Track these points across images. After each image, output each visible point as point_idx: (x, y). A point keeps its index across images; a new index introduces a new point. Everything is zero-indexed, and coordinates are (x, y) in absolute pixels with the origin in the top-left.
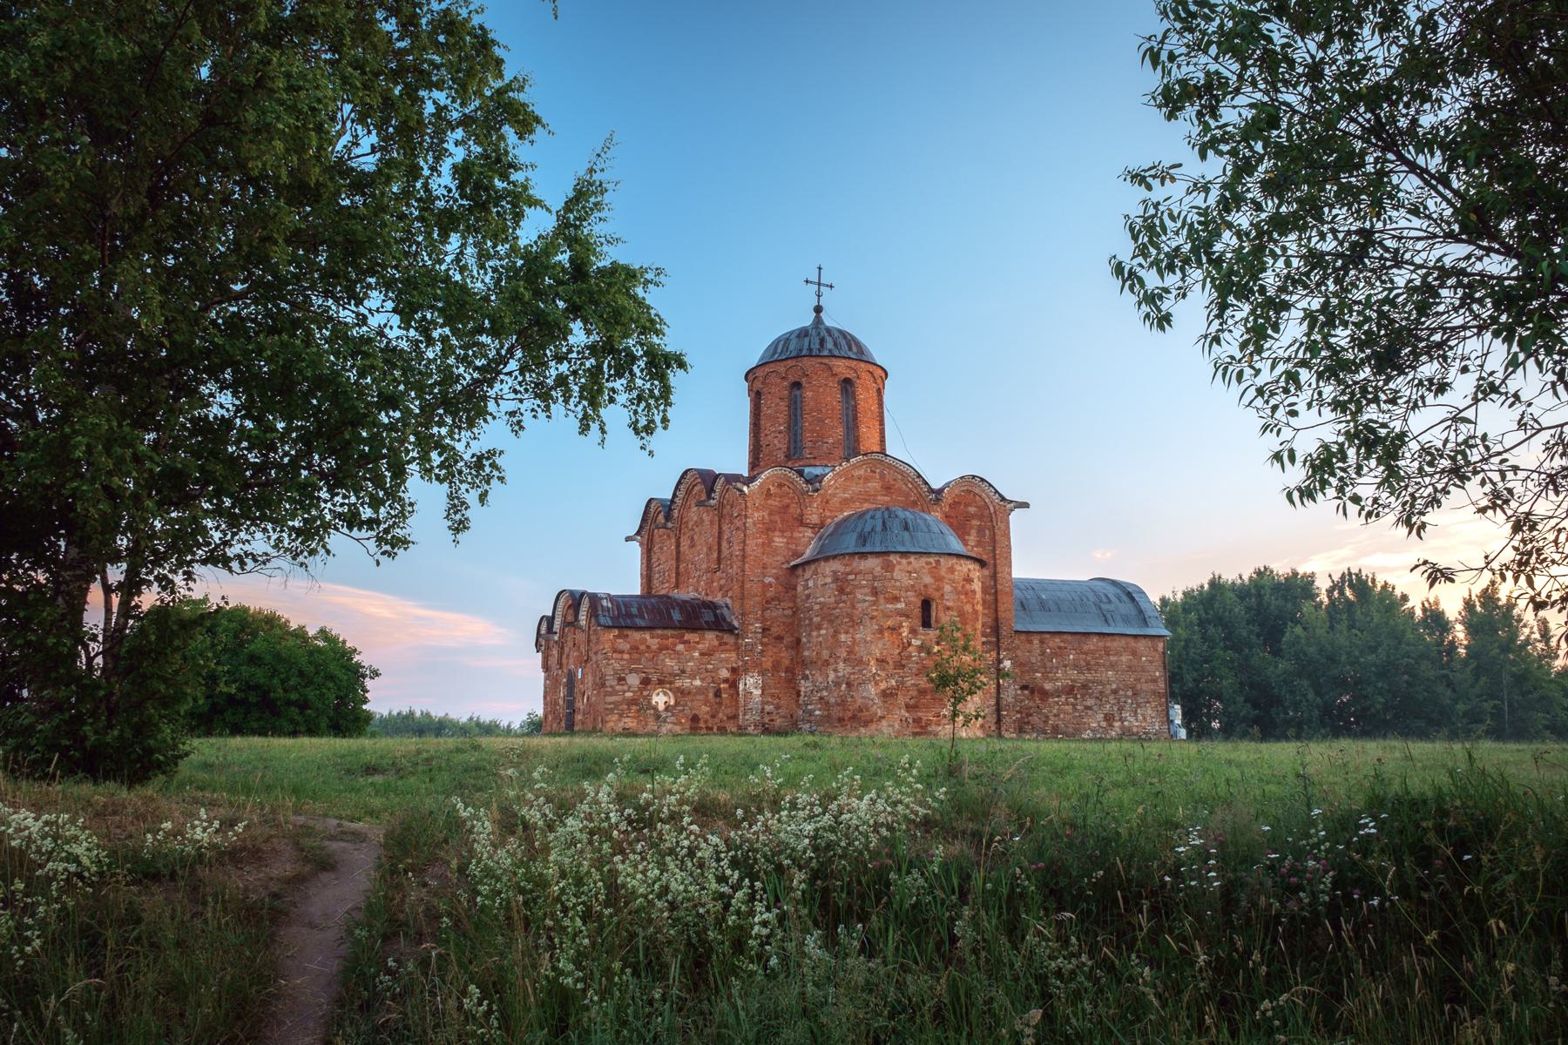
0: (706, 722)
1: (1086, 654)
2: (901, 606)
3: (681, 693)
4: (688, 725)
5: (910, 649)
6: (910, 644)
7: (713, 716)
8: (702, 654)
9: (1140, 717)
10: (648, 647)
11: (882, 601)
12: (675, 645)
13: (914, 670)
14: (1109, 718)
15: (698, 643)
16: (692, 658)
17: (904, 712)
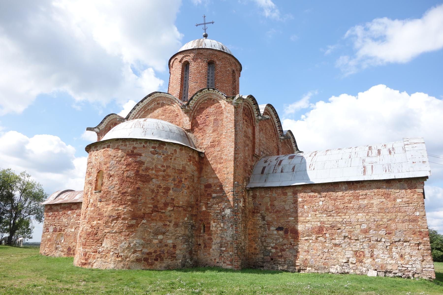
1: (335, 200)
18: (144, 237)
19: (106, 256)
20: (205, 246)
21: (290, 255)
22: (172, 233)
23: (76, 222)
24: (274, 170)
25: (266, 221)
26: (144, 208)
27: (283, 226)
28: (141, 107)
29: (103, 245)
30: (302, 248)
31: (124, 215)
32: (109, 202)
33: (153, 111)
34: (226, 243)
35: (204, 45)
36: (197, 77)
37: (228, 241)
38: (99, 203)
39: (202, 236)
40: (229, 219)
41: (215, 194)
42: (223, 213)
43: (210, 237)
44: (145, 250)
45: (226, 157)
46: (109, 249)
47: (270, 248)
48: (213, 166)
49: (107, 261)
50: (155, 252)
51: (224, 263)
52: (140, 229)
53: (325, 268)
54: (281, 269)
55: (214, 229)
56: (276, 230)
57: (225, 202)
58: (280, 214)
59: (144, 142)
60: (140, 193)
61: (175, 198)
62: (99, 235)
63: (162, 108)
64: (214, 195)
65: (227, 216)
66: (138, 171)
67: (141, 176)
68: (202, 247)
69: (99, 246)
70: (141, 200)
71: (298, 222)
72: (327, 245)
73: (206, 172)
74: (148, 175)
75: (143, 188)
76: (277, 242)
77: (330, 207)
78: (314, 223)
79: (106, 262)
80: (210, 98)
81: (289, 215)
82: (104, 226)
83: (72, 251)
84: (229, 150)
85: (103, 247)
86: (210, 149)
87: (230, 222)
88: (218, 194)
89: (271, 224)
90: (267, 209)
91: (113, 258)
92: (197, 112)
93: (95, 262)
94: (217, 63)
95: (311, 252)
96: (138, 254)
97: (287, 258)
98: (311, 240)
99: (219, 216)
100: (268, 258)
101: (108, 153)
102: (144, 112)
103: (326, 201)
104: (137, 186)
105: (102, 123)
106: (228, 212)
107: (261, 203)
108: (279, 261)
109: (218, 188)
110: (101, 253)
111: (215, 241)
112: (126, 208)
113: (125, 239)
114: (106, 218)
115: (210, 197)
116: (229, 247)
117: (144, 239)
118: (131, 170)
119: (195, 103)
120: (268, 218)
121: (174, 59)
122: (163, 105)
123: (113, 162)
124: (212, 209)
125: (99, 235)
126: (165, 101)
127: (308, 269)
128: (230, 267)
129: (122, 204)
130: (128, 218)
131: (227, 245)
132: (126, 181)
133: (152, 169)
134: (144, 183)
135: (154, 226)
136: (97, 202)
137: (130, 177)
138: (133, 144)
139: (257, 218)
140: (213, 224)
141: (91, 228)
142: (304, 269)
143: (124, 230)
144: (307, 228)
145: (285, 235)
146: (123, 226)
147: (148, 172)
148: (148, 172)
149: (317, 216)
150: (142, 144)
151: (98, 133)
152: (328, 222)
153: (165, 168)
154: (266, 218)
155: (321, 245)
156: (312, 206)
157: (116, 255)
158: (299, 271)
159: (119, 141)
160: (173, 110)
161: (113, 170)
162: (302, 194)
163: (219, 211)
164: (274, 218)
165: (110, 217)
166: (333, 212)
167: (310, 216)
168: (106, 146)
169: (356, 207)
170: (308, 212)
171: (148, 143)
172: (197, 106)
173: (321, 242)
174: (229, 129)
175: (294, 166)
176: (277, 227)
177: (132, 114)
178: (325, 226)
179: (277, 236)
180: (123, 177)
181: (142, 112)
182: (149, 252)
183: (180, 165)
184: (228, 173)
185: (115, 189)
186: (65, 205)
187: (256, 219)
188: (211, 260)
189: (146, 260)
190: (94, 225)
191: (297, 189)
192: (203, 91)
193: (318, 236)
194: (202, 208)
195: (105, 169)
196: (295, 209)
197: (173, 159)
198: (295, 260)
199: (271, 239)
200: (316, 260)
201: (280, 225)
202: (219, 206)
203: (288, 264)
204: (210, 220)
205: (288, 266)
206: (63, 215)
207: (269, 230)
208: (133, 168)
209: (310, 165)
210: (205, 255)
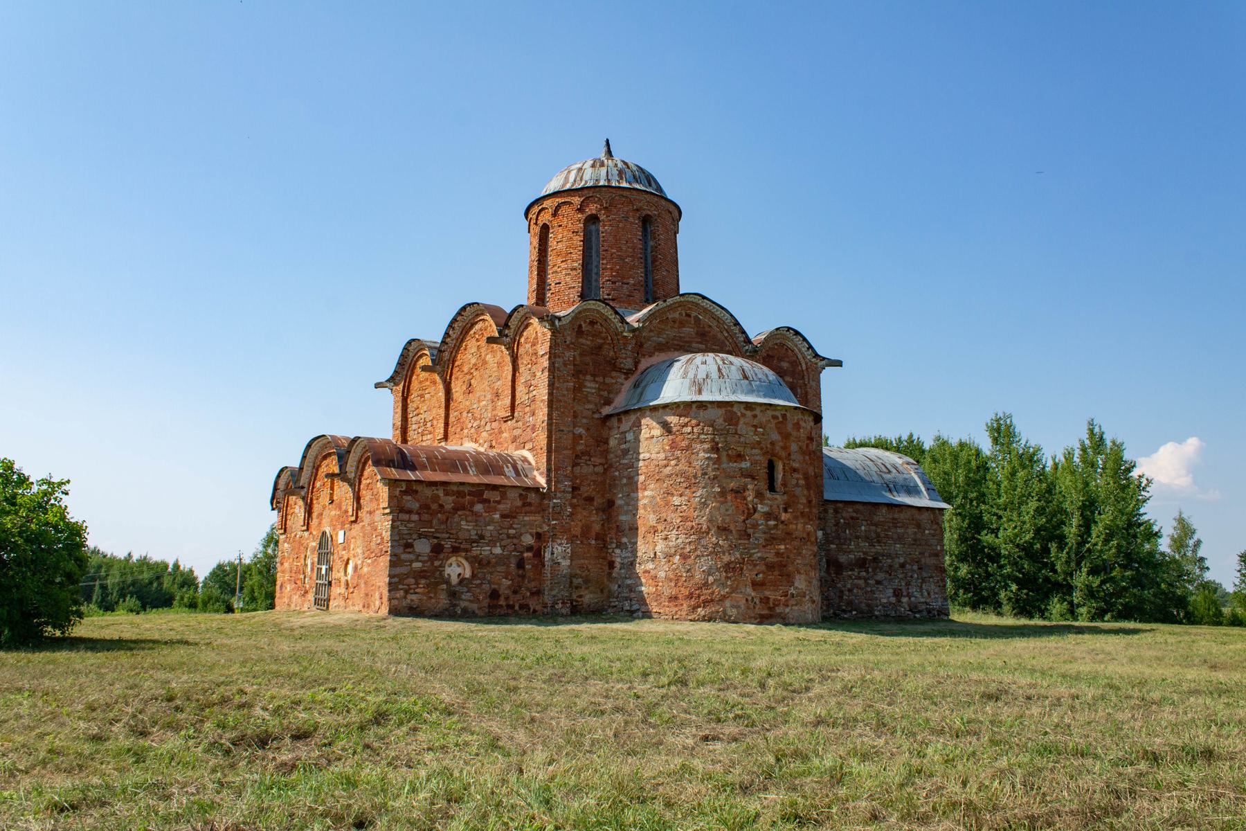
0: (507, 598)
1: (876, 525)
2: (745, 465)
3: (477, 562)
4: (486, 602)
5: (756, 516)
6: (755, 510)
7: (515, 592)
8: (503, 516)
9: (926, 594)
10: (441, 506)
11: (724, 459)
12: (472, 504)
14: (897, 593)
15: (499, 502)
16: (492, 521)
38: (783, 514)
83: (502, 598)
167: (853, 543)
169: (895, 536)
170: (850, 540)
186: (461, 488)
206: (459, 513)
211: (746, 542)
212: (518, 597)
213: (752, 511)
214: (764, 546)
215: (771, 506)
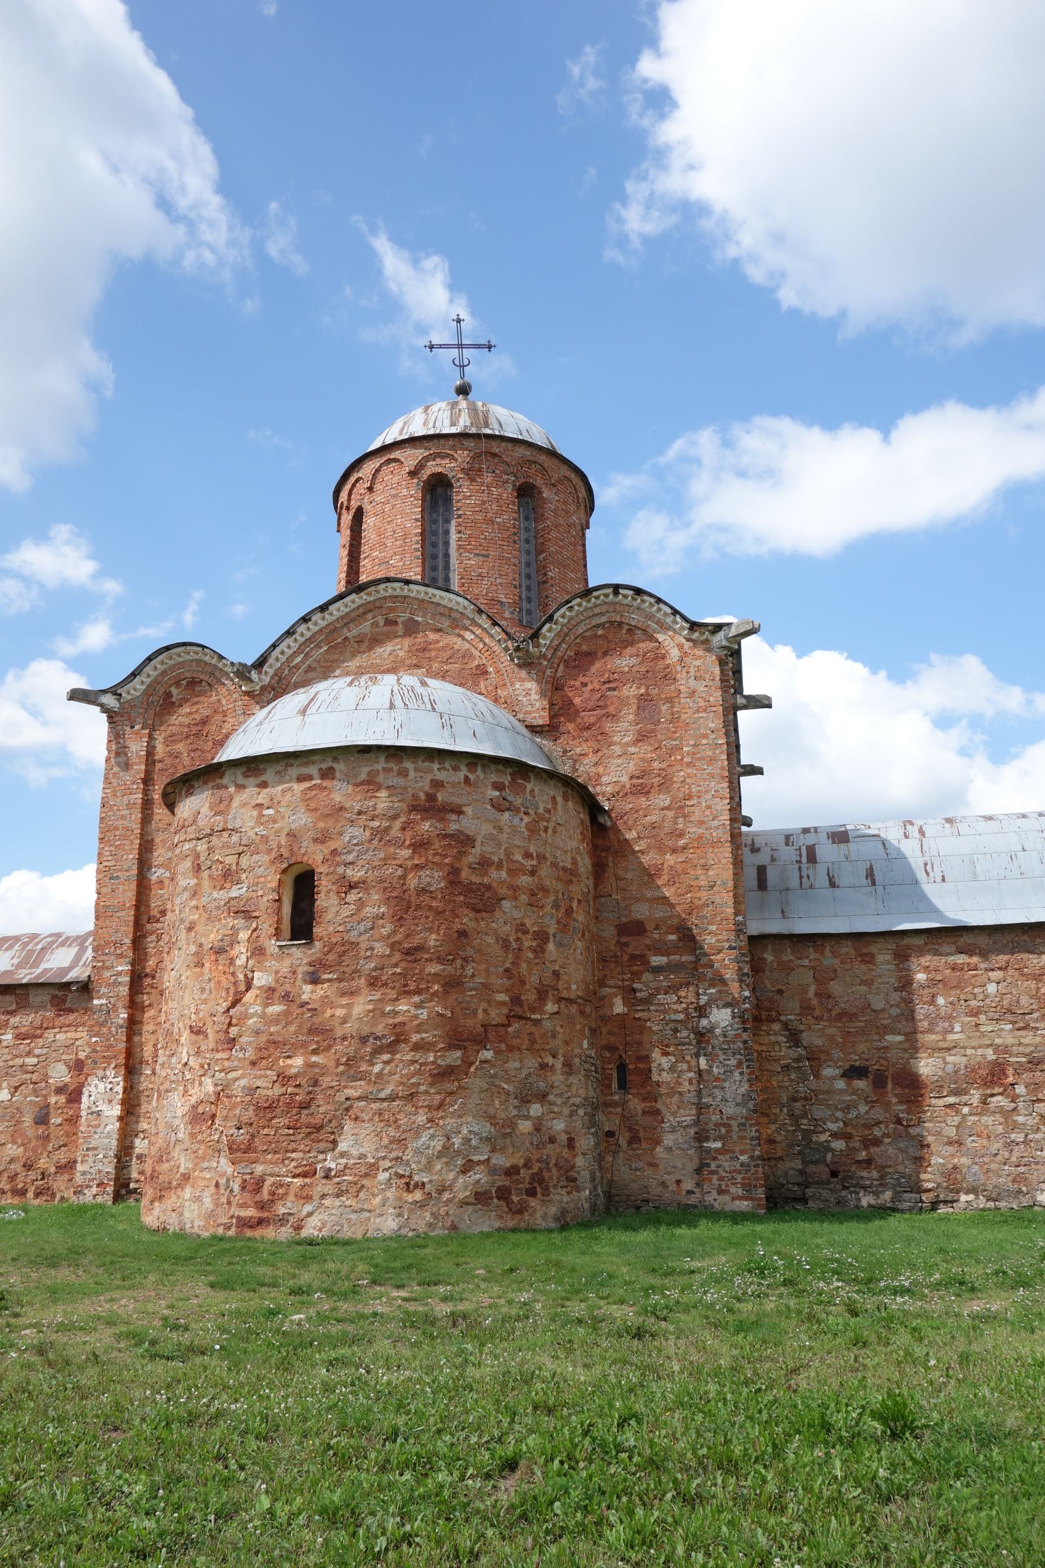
5: (249, 997)
7: (28, 1166)
8: (18, 1037)
11: (206, 884)
13: (250, 1054)
17: (225, 1165)
18: (491, 1110)
19: (363, 1186)
20: (634, 1139)
21: (898, 1157)
22: (561, 1095)
23: (18, 1061)
24: (801, 877)
25: (805, 1048)
26: (484, 1005)
27: (868, 1063)
28: (315, 629)
29: (342, 1146)
30: (938, 1133)
31: (418, 1032)
32: (354, 983)
33: (370, 649)
34: (724, 1125)
35: (496, 426)
36: (485, 539)
37: (728, 1118)
38: (308, 988)
39: (615, 1104)
40: (728, 1043)
41: (663, 955)
42: (704, 1022)
43: (651, 1107)
44: (500, 1160)
45: (700, 831)
46: (372, 1161)
47: (823, 1138)
48: (646, 859)
49: (365, 1207)
50: (527, 1165)
51: (721, 1192)
52: (475, 1082)
53: (1020, 1191)
54: (870, 1206)
55: (666, 1077)
56: (842, 1076)
57: (707, 984)
58: (854, 1025)
59: (467, 765)
60: (470, 952)
61: (562, 971)
62: (322, 1109)
63: (407, 641)
64: (657, 960)
65: (718, 1031)
66: (455, 871)
67: (468, 889)
68: (623, 1142)
69: (322, 1152)
70: (473, 976)
71: (917, 1050)
72: (1020, 1119)
73: (618, 879)
74: (489, 887)
75: (478, 933)
76: (850, 1116)
77: (1025, 1001)
78: (973, 1051)
79: (362, 1210)
80: (618, 619)
81: (885, 1027)
82: (343, 1073)
84: (709, 807)
85: (343, 1155)
86: (630, 798)
87: (734, 1054)
88: (672, 957)
89: (823, 1057)
90: (806, 1009)
91: (391, 1194)
92: (566, 667)
93: (310, 1214)
94: (545, 495)
95: (969, 1145)
96: (478, 1175)
97: (890, 1166)
98: (965, 1104)
99: (685, 1033)
100: (823, 1171)
101: (332, 796)
102: (326, 648)
103: (1009, 980)
104: (457, 926)
105: (134, 675)
106: (721, 1017)
107: (784, 988)
108: (862, 1178)
109: (673, 937)
110: (335, 1176)
111: (671, 1119)
112: (424, 1008)
113: (430, 1120)
114: (349, 1046)
115: (640, 968)
116: (735, 1137)
117: (491, 1118)
118: (430, 865)
119: (558, 635)
120: (813, 1038)
121: (385, 459)
122: (411, 629)
123: (355, 833)
124: (652, 1008)
125: (322, 1109)
126: (421, 614)
127: (964, 1198)
128: (745, 1205)
129: (408, 993)
130: (433, 1044)
131: (728, 1132)
132: (418, 907)
133: (499, 866)
134: (479, 915)
135: (516, 1069)
136: (299, 982)
137: (431, 892)
138: (431, 771)
139: (773, 1038)
140: (660, 1060)
141: (277, 1084)
142: (949, 1199)
143: (423, 1088)
144: (950, 1068)
145: (875, 1094)
146: (418, 1072)
147: (486, 874)
148: (486, 874)
149: (983, 1029)
150: (460, 770)
151: (112, 716)
152: (1021, 1049)
153: (534, 863)
154: (806, 1038)
155: (1002, 1120)
156: (963, 997)
157: (403, 1181)
158: (934, 1206)
159: (372, 755)
160: (458, 650)
161: (360, 863)
162: (926, 960)
163: (681, 1017)
164: (831, 1038)
165: (364, 1040)
166: (1035, 1015)
167: (957, 1028)
168: (313, 770)
170: (950, 1018)
171: (479, 768)
172: (564, 646)
173: (1001, 1110)
174: (705, 736)
175: (871, 869)
176: (847, 1067)
177: (278, 650)
178: (1011, 1060)
179: (849, 1098)
180: (405, 891)
181: (318, 646)
182: (511, 1167)
183: (566, 852)
184: (712, 887)
185: (377, 936)
187: (766, 1041)
188: (664, 1185)
189: (503, 1194)
190: (294, 1071)
191: (906, 941)
192: (595, 594)
193: (989, 1092)
194: (612, 1005)
195: (319, 858)
196: (906, 1006)
197: (550, 831)
198: (919, 1173)
199: (828, 1106)
200: (988, 1171)
201: (856, 1061)
202: (679, 998)
203: (893, 1187)
204: (648, 1045)
205: (896, 1193)
207: (817, 1076)
208: (437, 859)
209: (926, 865)
210: (636, 1169)
211: (225, 1055)
212: (32, 1176)
213: (242, 988)
214: (253, 1064)
215: (277, 972)
